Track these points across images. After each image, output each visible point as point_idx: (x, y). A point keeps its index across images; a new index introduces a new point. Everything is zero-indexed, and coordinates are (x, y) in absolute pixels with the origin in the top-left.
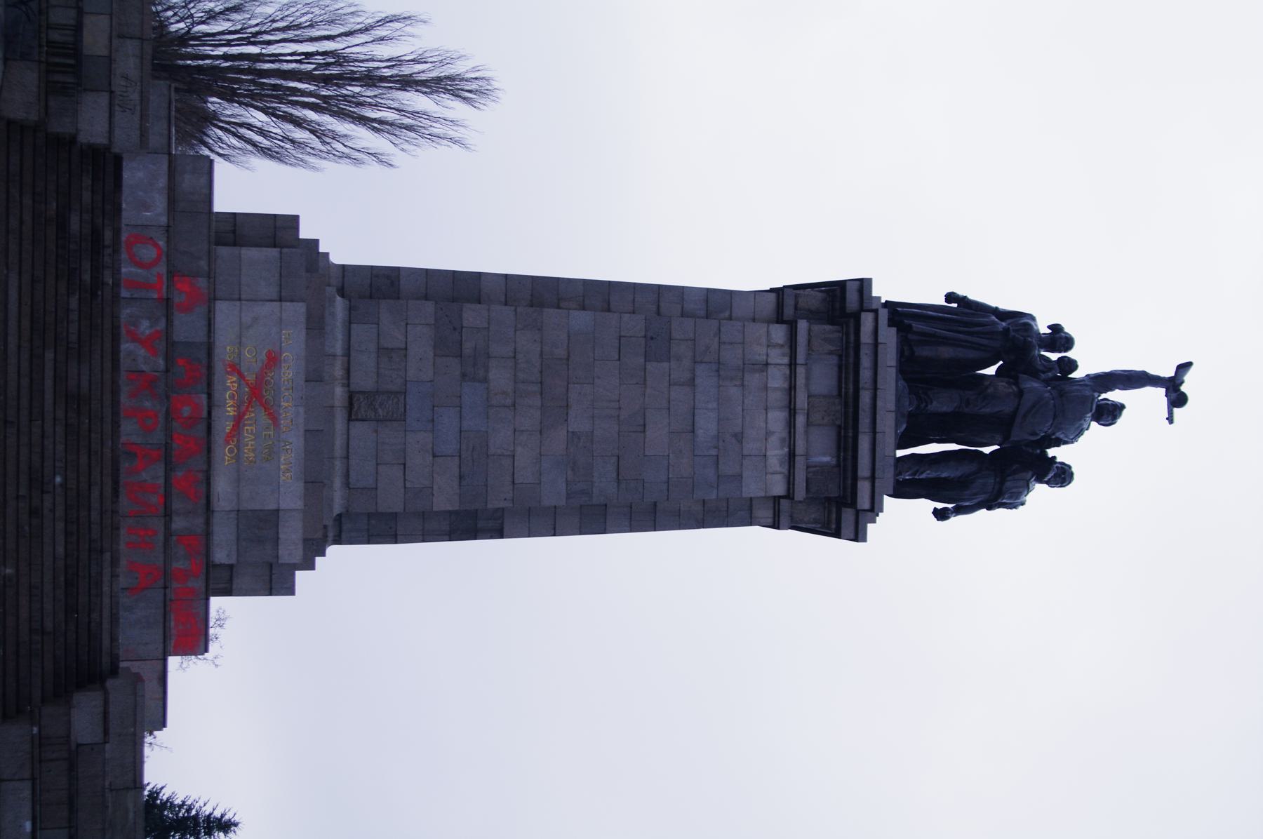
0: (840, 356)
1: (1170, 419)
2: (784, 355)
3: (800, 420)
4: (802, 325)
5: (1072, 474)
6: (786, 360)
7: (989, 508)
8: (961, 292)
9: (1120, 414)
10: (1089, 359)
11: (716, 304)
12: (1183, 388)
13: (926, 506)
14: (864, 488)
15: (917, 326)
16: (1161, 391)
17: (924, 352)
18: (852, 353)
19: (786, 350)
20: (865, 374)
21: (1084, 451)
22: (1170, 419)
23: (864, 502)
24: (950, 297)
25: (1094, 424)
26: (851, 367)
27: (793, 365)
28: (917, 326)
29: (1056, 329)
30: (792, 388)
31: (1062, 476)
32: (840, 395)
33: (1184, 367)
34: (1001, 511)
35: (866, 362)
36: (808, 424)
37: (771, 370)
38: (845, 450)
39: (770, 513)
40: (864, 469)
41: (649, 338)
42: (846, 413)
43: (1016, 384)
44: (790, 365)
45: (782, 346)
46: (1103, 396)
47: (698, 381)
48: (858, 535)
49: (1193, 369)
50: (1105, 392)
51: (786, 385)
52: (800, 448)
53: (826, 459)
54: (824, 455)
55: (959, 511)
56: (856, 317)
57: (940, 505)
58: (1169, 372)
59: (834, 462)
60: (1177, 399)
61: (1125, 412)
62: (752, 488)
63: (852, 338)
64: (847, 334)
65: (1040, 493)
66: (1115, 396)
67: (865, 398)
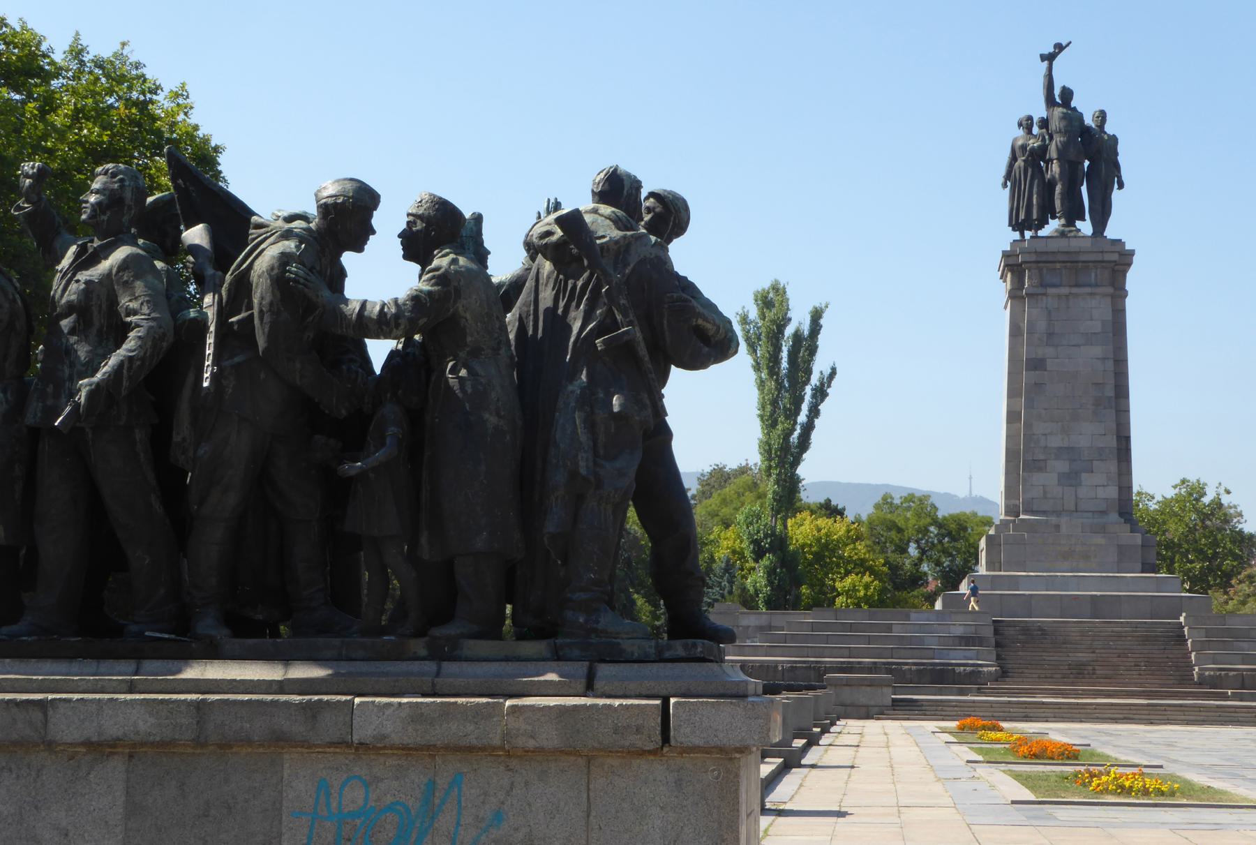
7: (1117, 154)
8: (1002, 180)
10: (1039, 110)
11: (1015, 332)
12: (1052, 50)
13: (1116, 196)
14: (1107, 257)
15: (1022, 216)
16: (1054, 63)
21: (1086, 106)
23: (1115, 257)
24: (1005, 185)
25: (1073, 104)
28: (1022, 216)
30: (1059, 296)
34: (1120, 148)
35: (1044, 258)
36: (1077, 285)
41: (1035, 369)
46: (1058, 100)
48: (1132, 253)
55: (1120, 178)
57: (1116, 186)
60: (1060, 48)
62: (1108, 316)
65: (1109, 129)
66: (1057, 92)
67: (1061, 258)
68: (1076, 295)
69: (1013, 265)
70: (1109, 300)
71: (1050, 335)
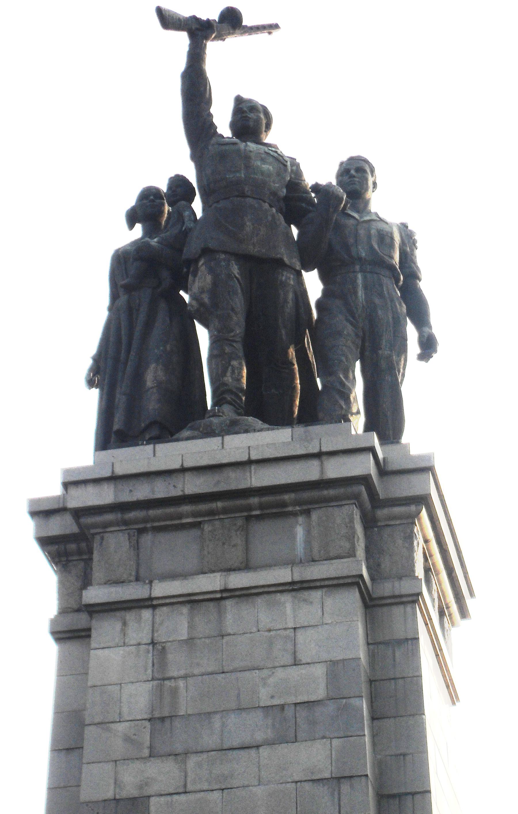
0: (141, 531)
1: (271, 28)
2: (139, 620)
3: (239, 580)
4: (95, 594)
5: (351, 159)
6: (146, 614)
9: (250, 101)
14: (335, 469)
17: (152, 405)
18: (132, 515)
19: (130, 616)
20: (161, 490)
22: (271, 28)
26: (152, 513)
27: (149, 603)
29: (132, 218)
30: (192, 601)
31: (355, 175)
32: (196, 525)
33: (167, 20)
35: (142, 492)
36: (246, 566)
37: (161, 636)
38: (284, 505)
39: (398, 611)
40: (310, 472)
42: (225, 511)
43: (197, 261)
44: (154, 607)
45: (125, 624)
47: (179, 748)
49: (166, 6)
50: (212, 126)
51: (185, 610)
52: (283, 575)
53: (300, 532)
54: (293, 537)
55: (421, 318)
56: (78, 513)
58: (182, 40)
59: (301, 519)
61: (246, 96)
63: (109, 517)
64: (106, 525)
67: (194, 485)
68: (246, 594)
69: (72, 536)
70: (352, 599)
71: (159, 721)
